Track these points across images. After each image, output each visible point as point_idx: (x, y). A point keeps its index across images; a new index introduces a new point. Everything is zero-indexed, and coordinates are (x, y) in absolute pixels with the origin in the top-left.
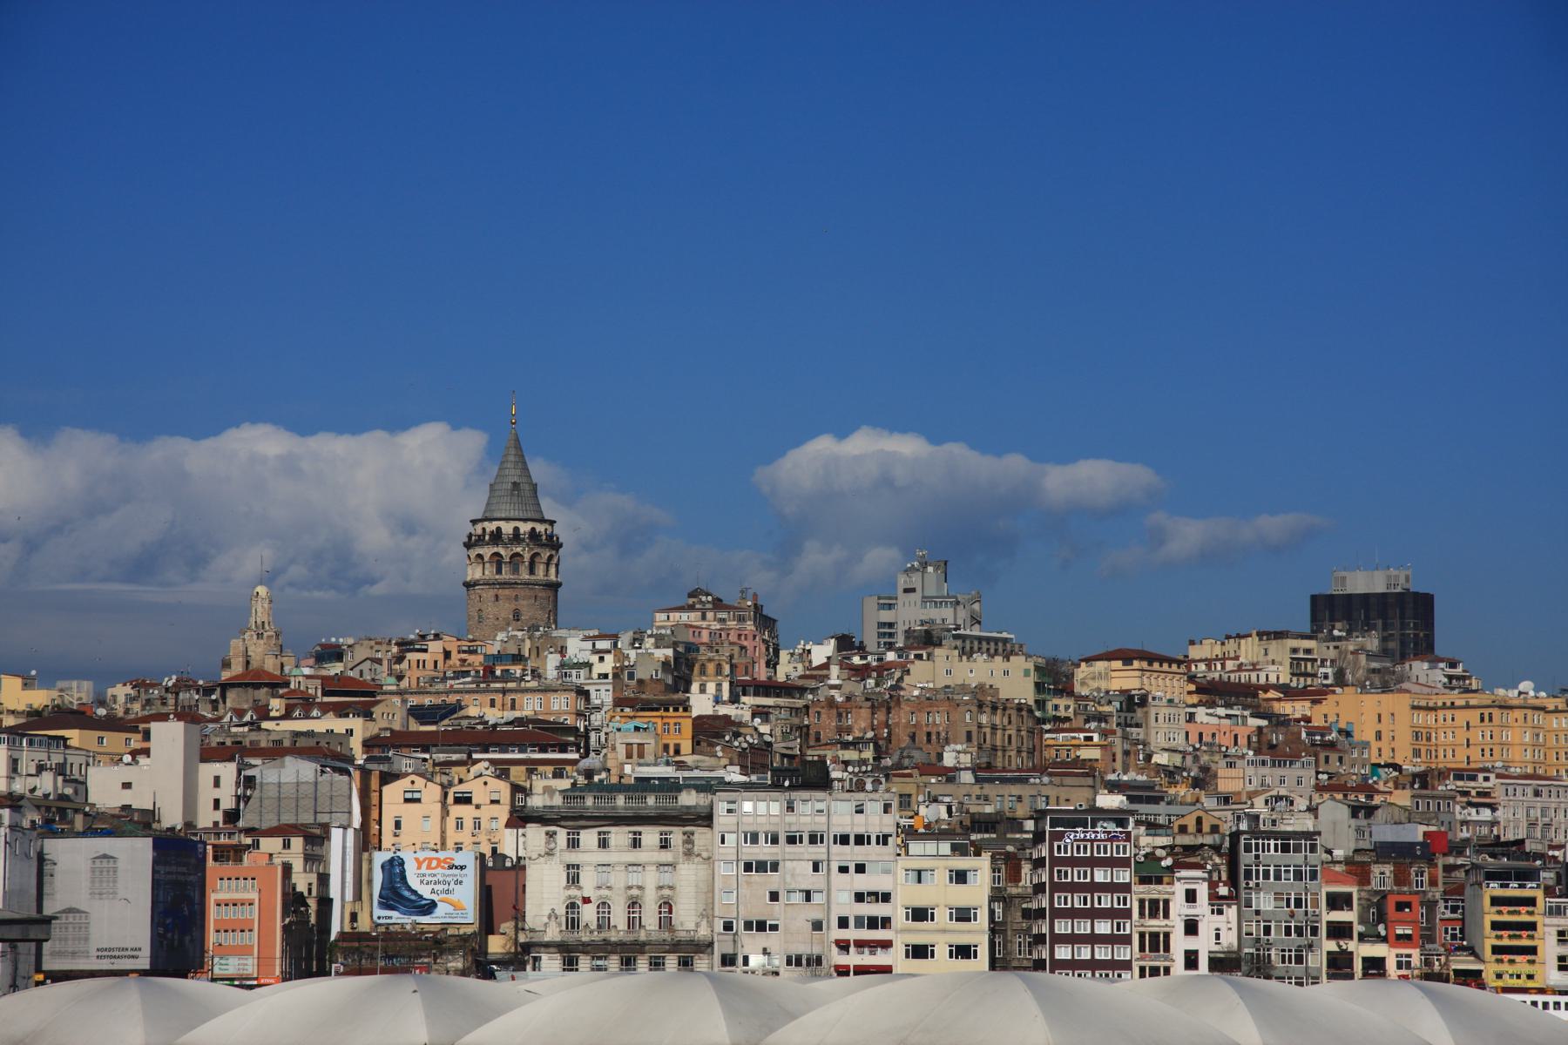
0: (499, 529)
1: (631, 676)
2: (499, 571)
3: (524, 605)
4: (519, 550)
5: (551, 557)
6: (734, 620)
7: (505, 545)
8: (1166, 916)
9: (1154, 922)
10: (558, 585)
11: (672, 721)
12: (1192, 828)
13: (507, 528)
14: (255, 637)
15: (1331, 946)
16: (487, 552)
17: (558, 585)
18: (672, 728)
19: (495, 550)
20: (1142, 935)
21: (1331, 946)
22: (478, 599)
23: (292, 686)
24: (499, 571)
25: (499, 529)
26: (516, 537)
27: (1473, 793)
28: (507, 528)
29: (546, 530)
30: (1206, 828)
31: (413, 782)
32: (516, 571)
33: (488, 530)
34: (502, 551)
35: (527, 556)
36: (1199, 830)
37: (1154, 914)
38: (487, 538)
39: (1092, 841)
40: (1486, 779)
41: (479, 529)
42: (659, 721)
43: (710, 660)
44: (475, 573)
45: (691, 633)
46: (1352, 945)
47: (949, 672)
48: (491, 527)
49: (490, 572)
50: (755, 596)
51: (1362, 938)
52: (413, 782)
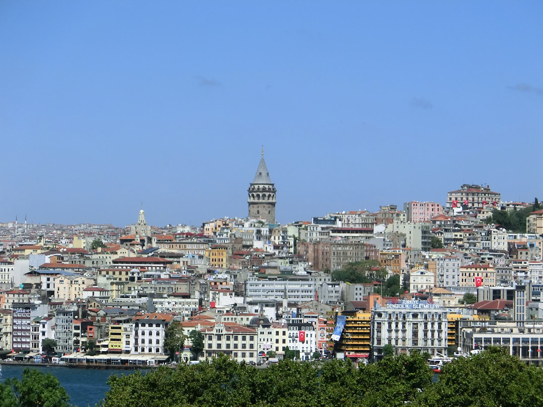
1: (235, 237)
3: (260, 209)
5: (274, 195)
7: (255, 192)
8: (38, 331)
9: (35, 332)
11: (221, 252)
12: (93, 306)
15: (75, 338)
18: (221, 254)
20: (33, 336)
21: (75, 338)
27: (520, 267)
30: (96, 306)
32: (259, 199)
34: (254, 193)
35: (261, 194)
36: (95, 307)
37: (35, 331)
39: (22, 313)
40: (525, 263)
42: (217, 252)
43: (277, 229)
44: (252, 200)
45: (413, 205)
46: (79, 338)
47: (398, 227)
50: (488, 186)
51: (82, 336)
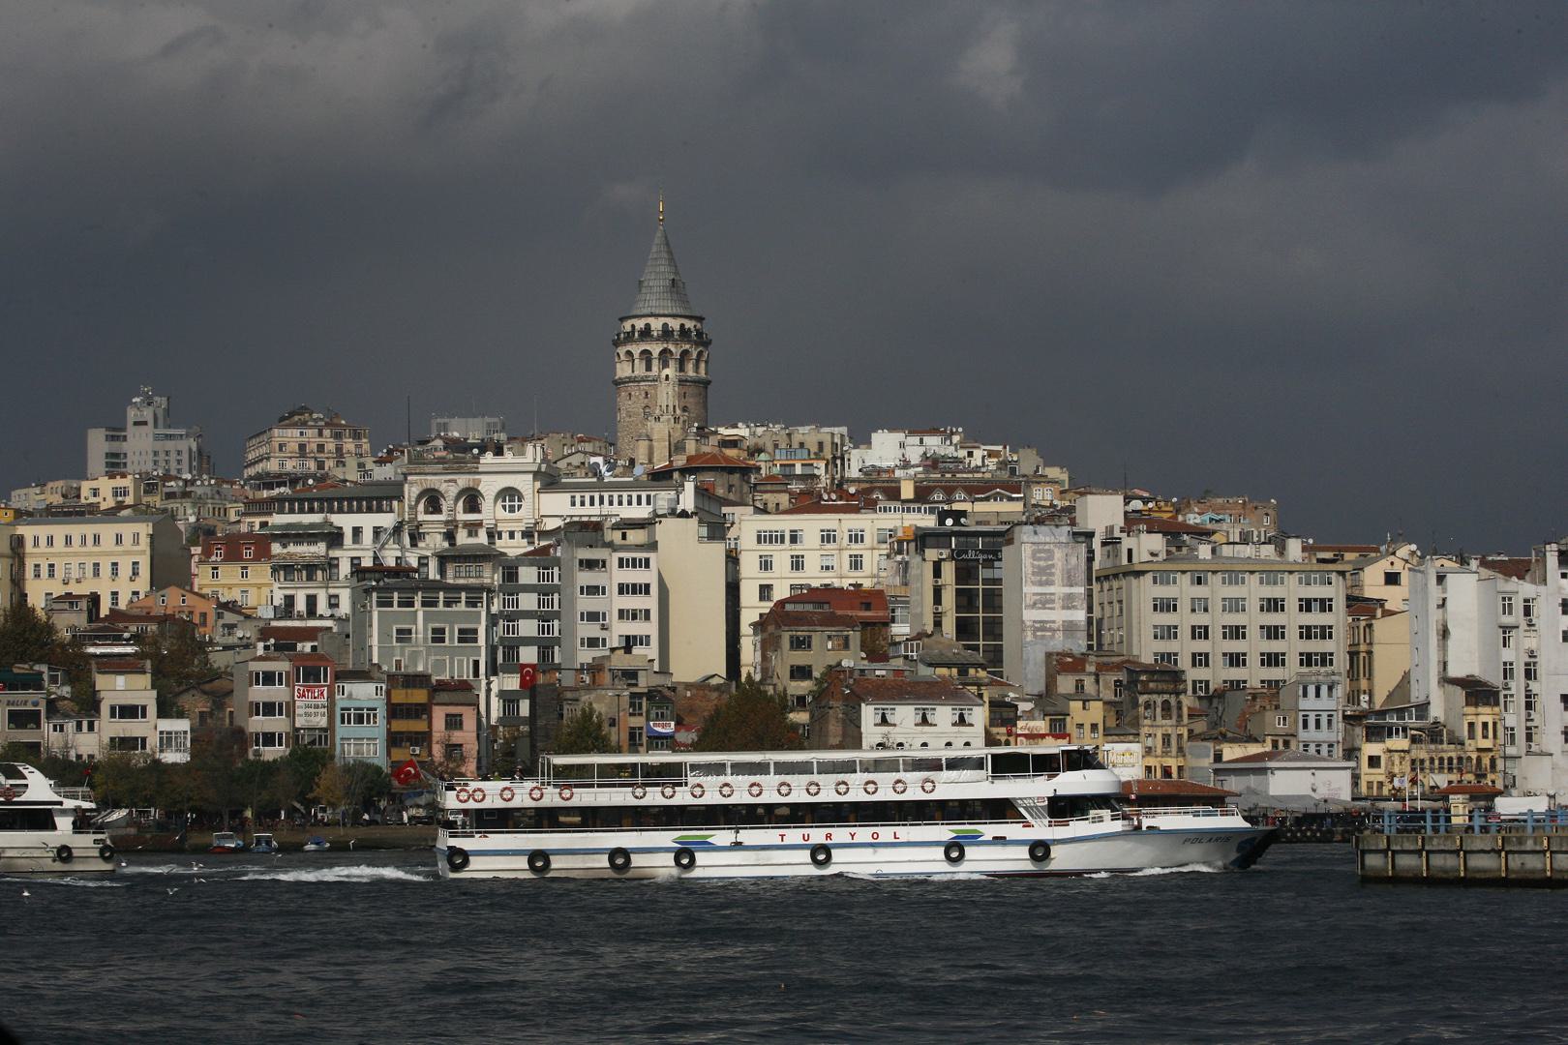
0: (648, 326)
2: (649, 368)
4: (687, 346)
6: (350, 437)
10: (708, 383)
13: (656, 324)
14: (673, 421)
16: (656, 349)
17: (708, 383)
19: (665, 346)
22: (644, 396)
23: (763, 472)
24: (649, 368)
25: (648, 326)
26: (684, 332)
28: (656, 324)
29: (695, 326)
31: (1392, 563)
33: (637, 328)
34: (672, 347)
38: (636, 335)
41: (627, 326)
48: (640, 324)
49: (640, 370)
52: (1392, 563)
